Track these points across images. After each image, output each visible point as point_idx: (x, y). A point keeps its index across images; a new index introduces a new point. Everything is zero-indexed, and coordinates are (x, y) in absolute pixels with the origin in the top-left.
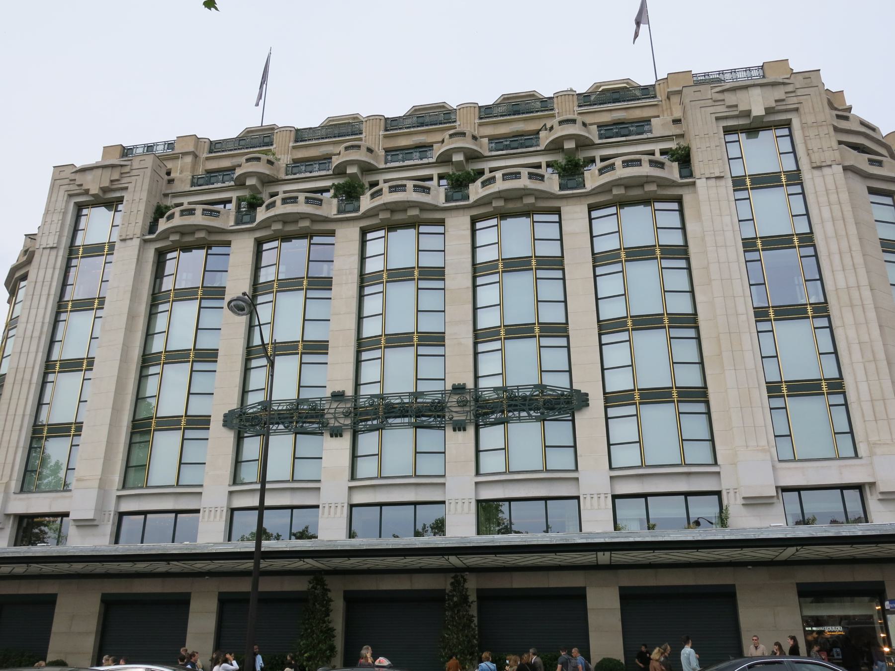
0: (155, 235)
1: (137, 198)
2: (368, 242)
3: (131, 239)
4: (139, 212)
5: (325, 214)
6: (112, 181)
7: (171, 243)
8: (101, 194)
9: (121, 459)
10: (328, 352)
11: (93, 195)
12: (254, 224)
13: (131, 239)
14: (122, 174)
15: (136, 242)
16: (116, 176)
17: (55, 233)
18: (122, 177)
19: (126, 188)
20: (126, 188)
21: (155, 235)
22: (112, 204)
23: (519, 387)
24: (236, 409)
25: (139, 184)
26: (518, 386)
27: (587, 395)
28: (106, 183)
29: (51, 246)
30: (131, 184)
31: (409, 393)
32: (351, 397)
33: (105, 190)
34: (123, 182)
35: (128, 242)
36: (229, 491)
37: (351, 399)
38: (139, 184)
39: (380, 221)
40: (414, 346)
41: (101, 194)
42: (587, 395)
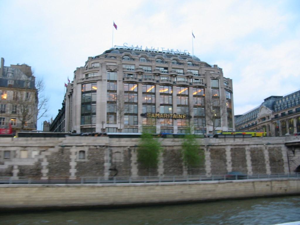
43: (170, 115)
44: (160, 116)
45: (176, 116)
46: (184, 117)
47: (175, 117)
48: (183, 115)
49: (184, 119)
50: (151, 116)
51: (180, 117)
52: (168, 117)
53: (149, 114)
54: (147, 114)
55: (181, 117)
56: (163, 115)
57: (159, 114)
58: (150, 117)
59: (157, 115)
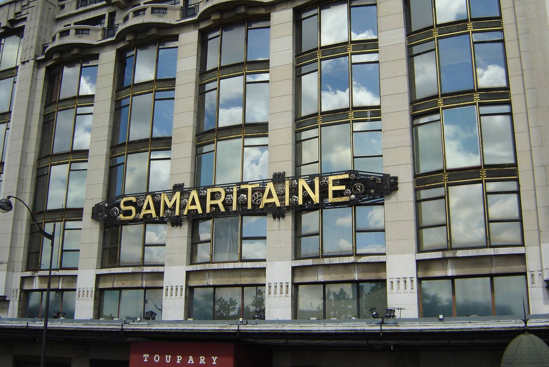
0: (115, 37)
1: (32, 26)
2: (303, 21)
3: (28, 61)
4: (34, 37)
5: (168, 22)
6: (16, 14)
7: (55, 61)
8: (9, 26)
9: (23, 246)
10: (268, 134)
11: (4, 28)
12: (196, 18)
13: (28, 61)
14: (23, 6)
15: (32, 63)
16: (18, 9)
17: (30, 48)
18: (23, 10)
19: (25, 19)
20: (25, 19)
21: (115, 37)
22: (19, 32)
23: (330, 174)
24: (100, 203)
25: (34, 14)
26: (331, 173)
27: (396, 178)
28: (12, 17)
29: (23, 61)
30: (28, 14)
31: (215, 187)
32: (188, 189)
33: (12, 22)
34: (23, 14)
35: (26, 64)
36: (21, 277)
37: (188, 191)
38: (34, 14)
39: (56, 61)
40: (318, 127)
41: (9, 26)
42: (396, 178)
43: (245, 191)
44: (182, 207)
45: (281, 196)
46: (336, 194)
47: (275, 199)
48: (331, 178)
49: (335, 205)
50: (139, 210)
51: (307, 198)
52: (227, 204)
53: (126, 204)
54: (118, 205)
55: (316, 197)
56: (203, 199)
57: (178, 195)
58: (135, 221)
59: (170, 205)
